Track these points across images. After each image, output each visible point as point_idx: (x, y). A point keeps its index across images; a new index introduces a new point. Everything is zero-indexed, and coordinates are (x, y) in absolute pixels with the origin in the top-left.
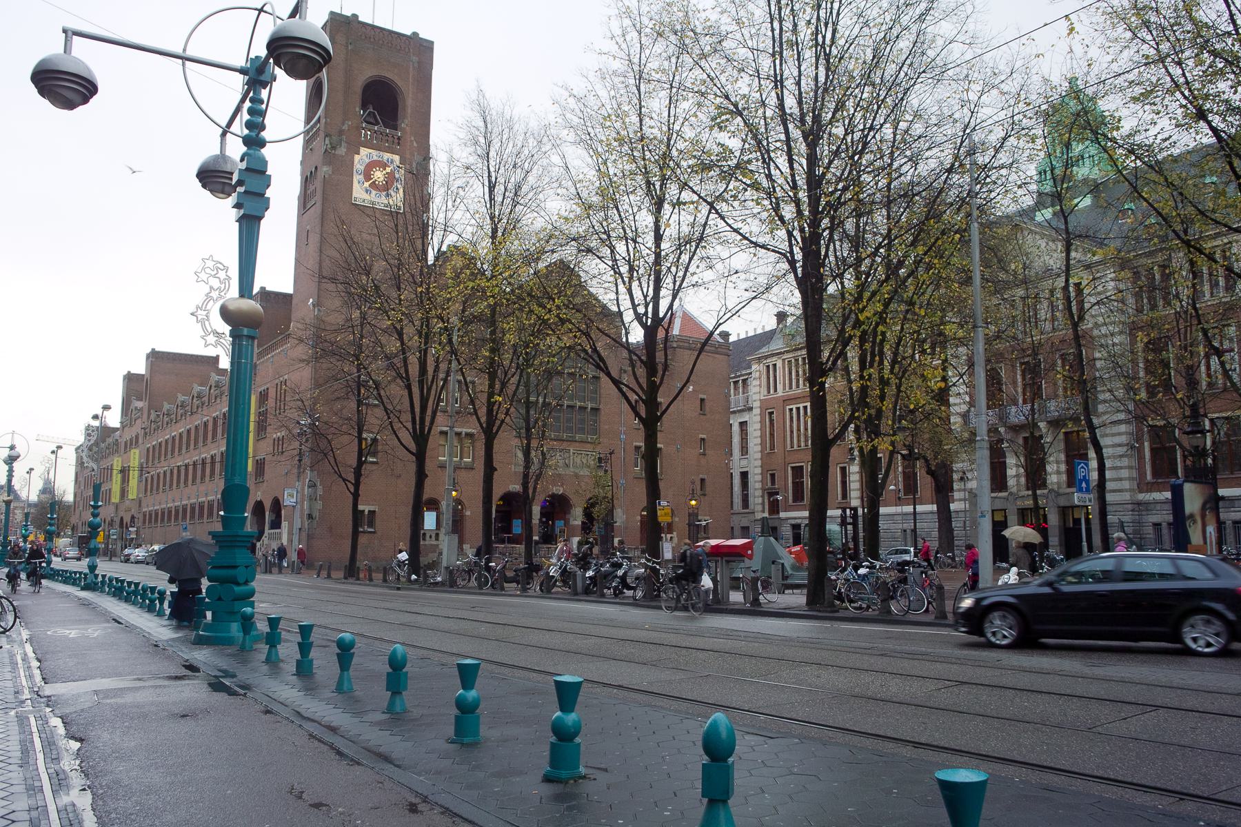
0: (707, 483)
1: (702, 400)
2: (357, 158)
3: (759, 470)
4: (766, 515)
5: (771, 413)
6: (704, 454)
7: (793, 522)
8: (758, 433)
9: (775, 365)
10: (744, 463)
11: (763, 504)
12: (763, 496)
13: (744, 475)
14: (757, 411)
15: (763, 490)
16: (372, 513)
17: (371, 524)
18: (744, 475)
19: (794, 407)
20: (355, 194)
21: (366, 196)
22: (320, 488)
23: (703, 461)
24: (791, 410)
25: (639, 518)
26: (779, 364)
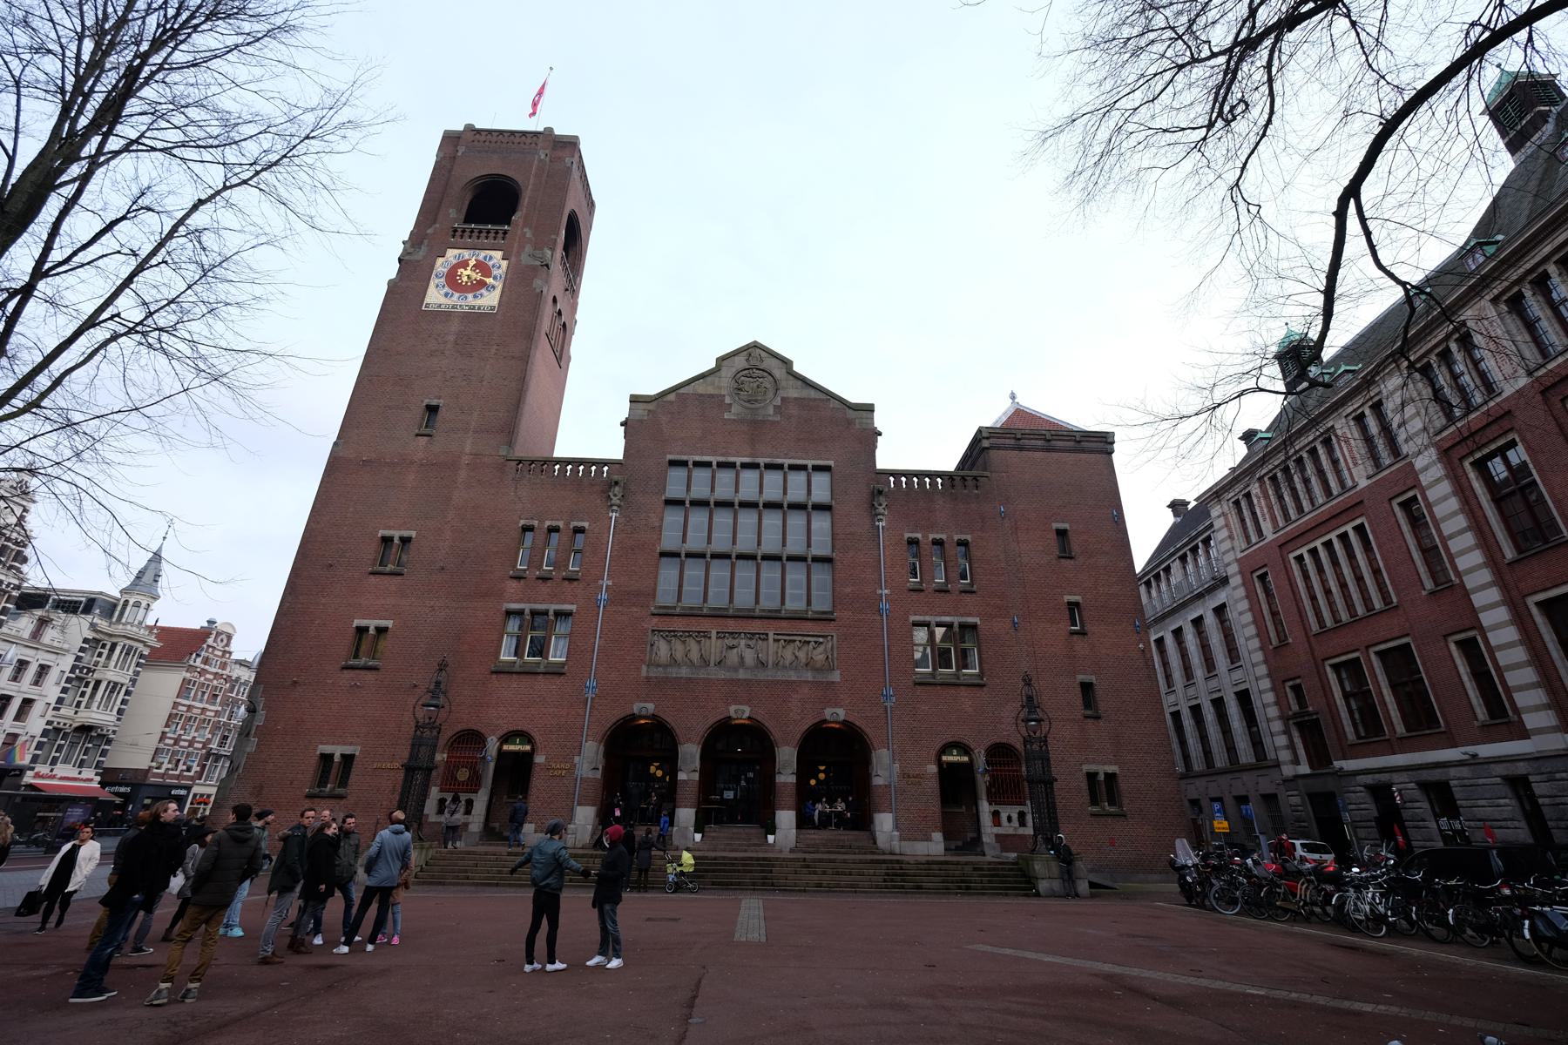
0: (1100, 692)
1: (1062, 533)
2: (440, 261)
3: (1266, 684)
4: (1304, 769)
5: (1263, 578)
6: (1082, 633)
7: (1369, 779)
8: (1248, 617)
9: (1248, 496)
10: (1237, 675)
11: (1291, 746)
12: (1287, 732)
13: (1244, 697)
14: (1236, 581)
15: (1284, 718)
16: (348, 759)
17: (344, 781)
18: (1244, 697)
19: (1304, 551)
20: (427, 300)
21: (443, 300)
22: (261, 714)
23: (1081, 646)
24: (1300, 559)
25: (933, 768)
26: (1255, 489)
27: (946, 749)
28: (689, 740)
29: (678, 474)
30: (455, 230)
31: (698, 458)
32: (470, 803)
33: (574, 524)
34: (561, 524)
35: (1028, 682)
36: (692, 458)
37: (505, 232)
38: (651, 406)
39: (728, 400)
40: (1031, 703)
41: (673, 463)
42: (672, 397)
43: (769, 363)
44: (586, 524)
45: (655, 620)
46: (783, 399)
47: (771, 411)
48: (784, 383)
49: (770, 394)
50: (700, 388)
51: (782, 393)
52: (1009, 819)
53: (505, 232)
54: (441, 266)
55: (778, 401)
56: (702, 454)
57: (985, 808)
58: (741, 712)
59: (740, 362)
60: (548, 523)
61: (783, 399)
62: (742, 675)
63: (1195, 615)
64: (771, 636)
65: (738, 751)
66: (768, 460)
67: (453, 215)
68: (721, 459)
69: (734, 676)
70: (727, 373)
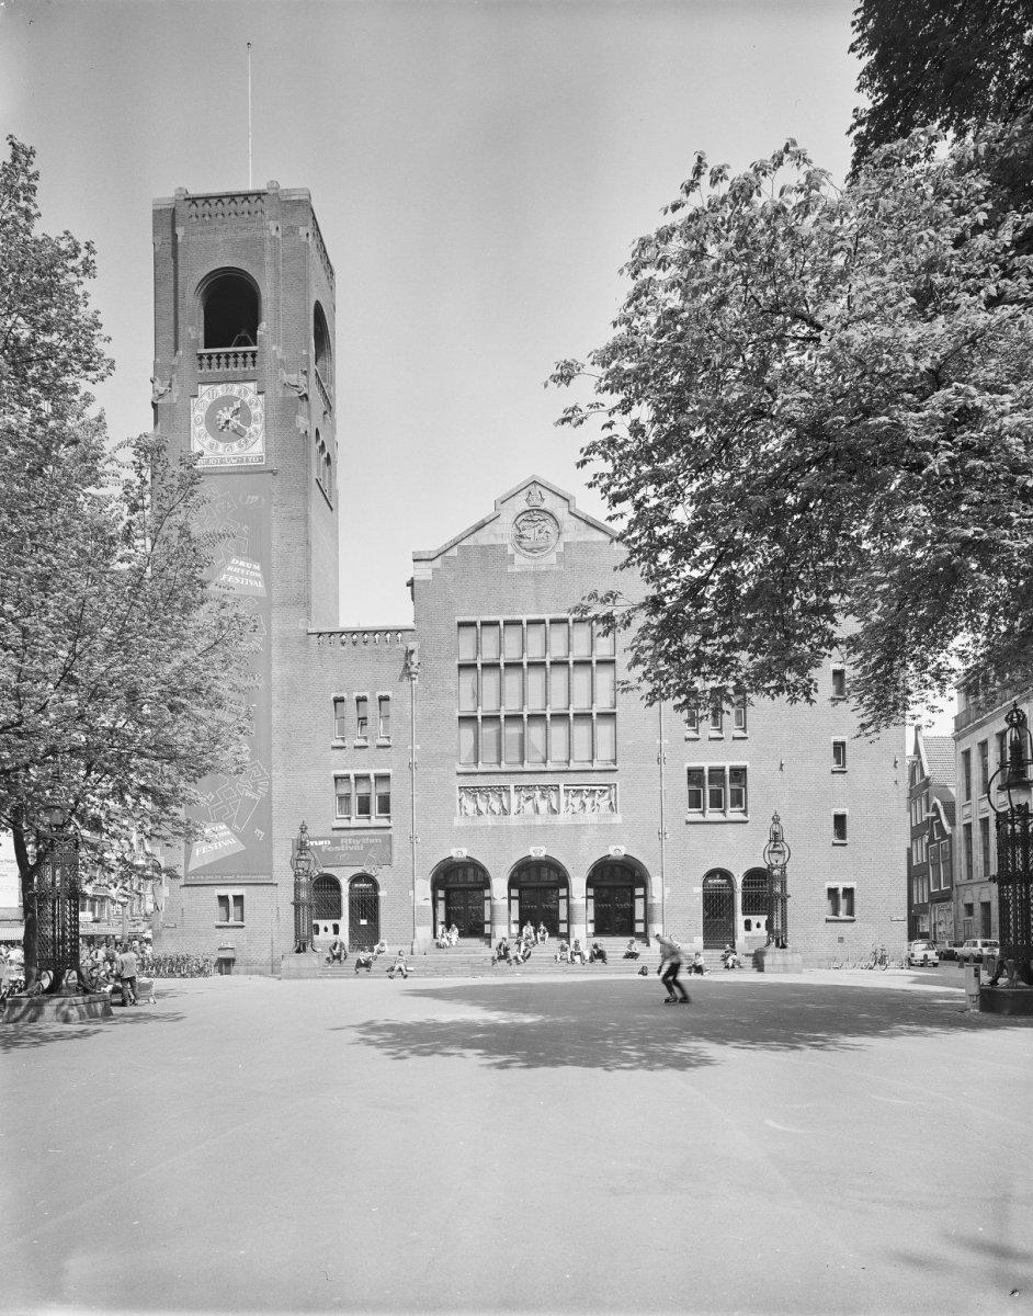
25: (699, 890)
27: (712, 874)
28: (498, 875)
29: (468, 636)
30: (201, 357)
31: (487, 618)
32: (336, 928)
33: (379, 694)
34: (367, 694)
35: (776, 820)
36: (479, 619)
37: (254, 354)
38: (438, 563)
39: (510, 551)
40: (776, 838)
41: (461, 625)
42: (454, 552)
43: (550, 503)
44: (389, 693)
45: (462, 778)
46: (566, 544)
47: (553, 558)
48: (566, 526)
49: (553, 541)
50: (483, 538)
51: (566, 538)
52: (758, 926)
53: (254, 354)
54: (198, 412)
55: (560, 548)
56: (489, 613)
57: (740, 919)
58: (538, 851)
59: (520, 504)
60: (356, 694)
61: (566, 544)
62: (539, 821)
63: (982, 739)
64: (562, 788)
65: (538, 888)
66: (553, 616)
67: (195, 331)
68: (509, 618)
69: (532, 822)
70: (508, 517)
